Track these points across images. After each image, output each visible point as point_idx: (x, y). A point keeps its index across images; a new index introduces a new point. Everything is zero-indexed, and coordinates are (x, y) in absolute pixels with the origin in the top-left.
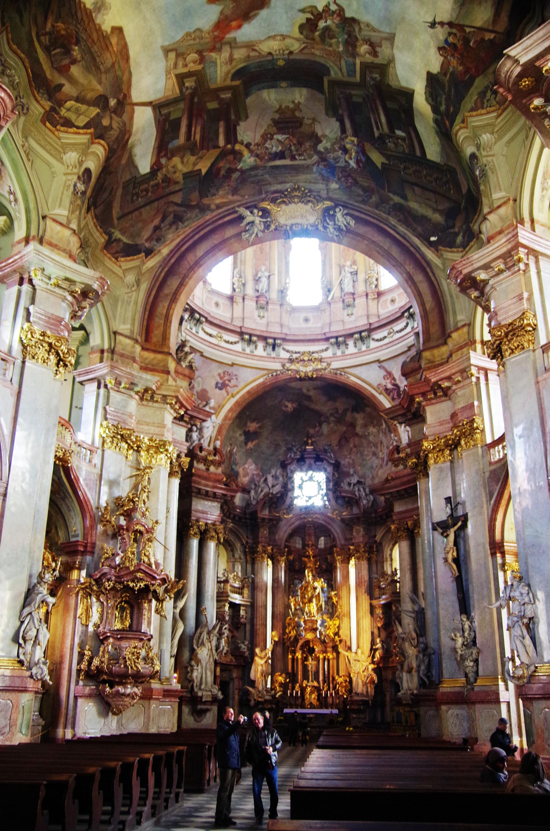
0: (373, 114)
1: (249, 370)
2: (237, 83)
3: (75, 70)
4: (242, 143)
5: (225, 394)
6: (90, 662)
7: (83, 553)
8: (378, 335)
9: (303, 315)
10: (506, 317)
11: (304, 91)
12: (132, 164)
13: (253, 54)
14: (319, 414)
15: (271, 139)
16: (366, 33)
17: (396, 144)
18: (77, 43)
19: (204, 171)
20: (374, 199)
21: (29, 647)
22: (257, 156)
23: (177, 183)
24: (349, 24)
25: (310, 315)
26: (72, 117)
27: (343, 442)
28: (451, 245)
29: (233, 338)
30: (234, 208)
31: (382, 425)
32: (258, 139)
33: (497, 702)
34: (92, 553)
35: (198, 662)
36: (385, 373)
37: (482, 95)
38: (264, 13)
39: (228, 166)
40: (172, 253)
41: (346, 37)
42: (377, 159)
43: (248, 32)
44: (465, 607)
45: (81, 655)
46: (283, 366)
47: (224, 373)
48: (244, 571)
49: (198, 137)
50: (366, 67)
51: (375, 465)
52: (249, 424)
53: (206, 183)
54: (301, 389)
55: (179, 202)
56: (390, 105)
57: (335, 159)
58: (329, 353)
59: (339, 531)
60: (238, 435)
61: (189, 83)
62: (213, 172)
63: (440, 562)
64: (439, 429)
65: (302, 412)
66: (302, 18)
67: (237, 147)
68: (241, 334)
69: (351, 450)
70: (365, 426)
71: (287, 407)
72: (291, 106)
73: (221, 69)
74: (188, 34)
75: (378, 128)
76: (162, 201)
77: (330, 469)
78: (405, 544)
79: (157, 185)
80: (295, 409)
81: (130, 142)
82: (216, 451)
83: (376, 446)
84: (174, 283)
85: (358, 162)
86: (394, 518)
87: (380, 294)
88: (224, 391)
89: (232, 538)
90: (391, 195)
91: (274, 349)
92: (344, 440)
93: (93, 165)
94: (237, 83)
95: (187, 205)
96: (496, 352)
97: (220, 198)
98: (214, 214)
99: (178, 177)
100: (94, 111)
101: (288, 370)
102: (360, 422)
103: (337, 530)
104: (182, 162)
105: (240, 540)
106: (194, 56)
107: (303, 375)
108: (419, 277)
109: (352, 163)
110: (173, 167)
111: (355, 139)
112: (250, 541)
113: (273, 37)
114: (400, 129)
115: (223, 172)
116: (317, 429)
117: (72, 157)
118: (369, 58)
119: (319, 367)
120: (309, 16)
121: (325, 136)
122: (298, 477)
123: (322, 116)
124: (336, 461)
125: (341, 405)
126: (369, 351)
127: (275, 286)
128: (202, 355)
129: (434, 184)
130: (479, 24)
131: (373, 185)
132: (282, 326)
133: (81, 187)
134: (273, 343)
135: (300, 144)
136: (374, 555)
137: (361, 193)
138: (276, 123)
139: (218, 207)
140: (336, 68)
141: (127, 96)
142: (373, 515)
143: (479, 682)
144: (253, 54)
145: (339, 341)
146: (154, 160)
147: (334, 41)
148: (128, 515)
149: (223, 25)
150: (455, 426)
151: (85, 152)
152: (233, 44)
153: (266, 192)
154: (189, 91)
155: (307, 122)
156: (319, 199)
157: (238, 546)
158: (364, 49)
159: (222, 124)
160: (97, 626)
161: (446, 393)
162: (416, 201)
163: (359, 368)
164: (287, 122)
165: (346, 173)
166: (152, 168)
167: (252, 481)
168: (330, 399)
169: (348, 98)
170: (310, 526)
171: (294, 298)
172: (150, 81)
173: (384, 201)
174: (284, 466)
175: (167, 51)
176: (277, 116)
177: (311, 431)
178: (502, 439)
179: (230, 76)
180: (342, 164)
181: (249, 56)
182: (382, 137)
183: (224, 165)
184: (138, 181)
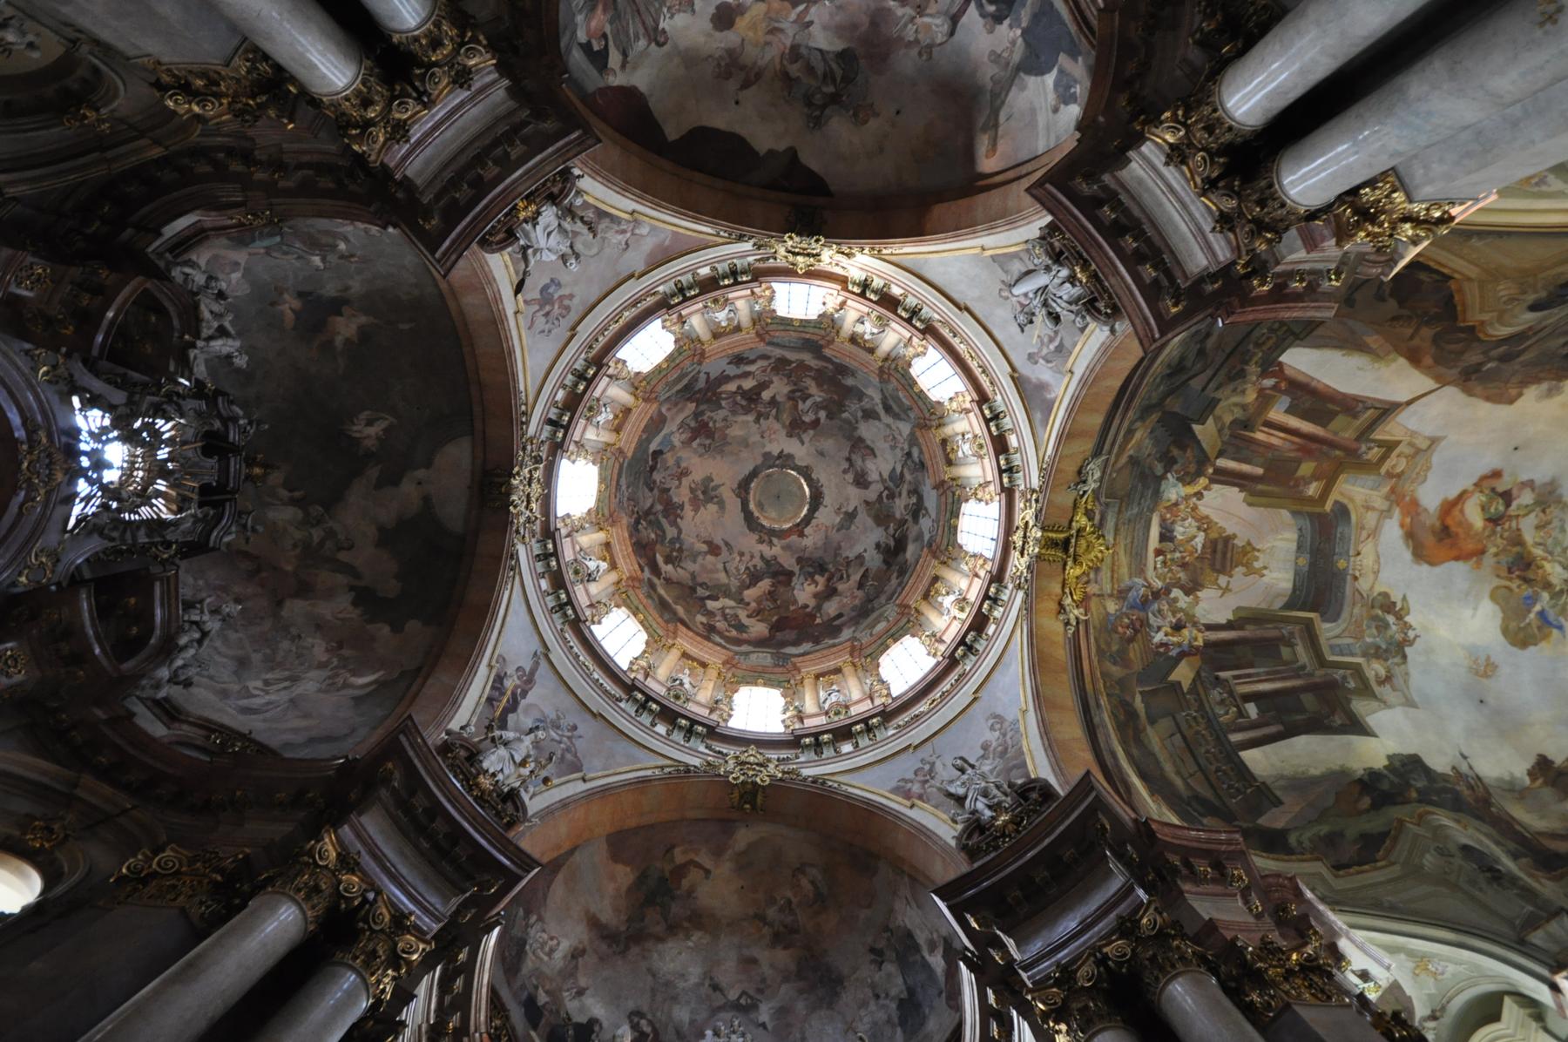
0: (1268, 673)
1: (547, 365)
2: (1328, 506)
4: (1206, 488)
5: (529, 297)
13: (1364, 534)
14: (333, 500)
15: (1199, 528)
16: (1397, 671)
17: (1222, 702)
19: (1196, 428)
20: (1116, 671)
22: (1176, 504)
23: (1217, 389)
24: (1398, 649)
30: (1110, 453)
31: (355, 674)
39: (1181, 461)
41: (1384, 646)
42: (1183, 674)
43: (1392, 531)
46: (531, 440)
47: (568, 308)
49: (1259, 436)
50: (1357, 670)
52: (363, 319)
54: (428, 464)
55: (1192, 382)
57: (1159, 611)
60: (351, 283)
66: (1396, 597)
67: (1203, 481)
70: (319, 626)
71: (370, 423)
72: (1257, 565)
74: (1429, 468)
75: (1236, 677)
79: (1247, 363)
81: (1402, 361)
85: (1162, 645)
86: (346, 830)
90: (1138, 699)
91: (550, 422)
94: (1328, 506)
97: (1142, 439)
98: (1126, 424)
99: (1218, 395)
101: (524, 449)
102: (326, 610)
104: (1236, 405)
106: (1402, 465)
107: (515, 482)
109: (1159, 637)
110: (1243, 392)
111: (1200, 643)
114: (1261, 711)
115: (1175, 452)
116: (284, 493)
118: (1370, 674)
120: (1399, 606)
121: (1197, 600)
124: (213, 549)
128: (632, 276)
129: (1213, 768)
131: (1138, 666)
135: (1184, 566)
137: (1115, 648)
138: (1228, 540)
139: (1130, 432)
140: (1337, 631)
144: (1364, 534)
146: (1287, 372)
147: (1374, 631)
149: (1412, 508)
152: (1386, 514)
153: (1107, 505)
154: (1364, 448)
155: (1223, 580)
159: (1260, 471)
162: (1162, 740)
163: (524, 607)
164: (1223, 554)
165: (1141, 628)
166: (1280, 364)
168: (381, 529)
173: (1121, 682)
175: (1434, 441)
176: (1239, 542)
177: (276, 477)
179: (1345, 501)
180: (1152, 620)
181: (1363, 528)
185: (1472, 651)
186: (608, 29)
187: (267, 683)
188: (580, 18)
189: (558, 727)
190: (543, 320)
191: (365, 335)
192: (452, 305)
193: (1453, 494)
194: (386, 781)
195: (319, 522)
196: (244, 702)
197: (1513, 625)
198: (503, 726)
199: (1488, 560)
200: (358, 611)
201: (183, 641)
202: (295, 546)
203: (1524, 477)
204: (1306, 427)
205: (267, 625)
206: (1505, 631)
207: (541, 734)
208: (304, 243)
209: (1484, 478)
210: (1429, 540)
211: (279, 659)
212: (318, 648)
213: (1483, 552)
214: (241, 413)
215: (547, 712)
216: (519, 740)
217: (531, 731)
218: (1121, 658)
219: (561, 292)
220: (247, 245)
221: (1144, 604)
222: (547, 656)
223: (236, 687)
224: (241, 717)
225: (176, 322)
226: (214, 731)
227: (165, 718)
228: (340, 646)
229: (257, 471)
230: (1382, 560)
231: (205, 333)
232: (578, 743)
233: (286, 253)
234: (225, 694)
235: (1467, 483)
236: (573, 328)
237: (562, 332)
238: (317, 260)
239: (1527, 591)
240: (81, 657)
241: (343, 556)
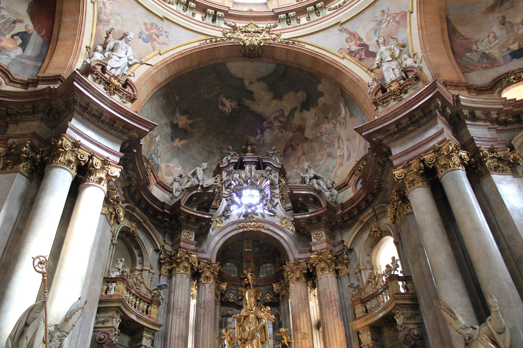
1: (183, 30)
14: (260, 118)
27: (289, 151)
31: (340, 114)
36: (348, 36)
46: (224, 34)
47: (152, 24)
51: (331, 168)
52: (178, 115)
54: (242, 80)
59: (292, 243)
60: (163, 123)
69: (299, 158)
70: (317, 125)
71: (224, 105)
77: (275, 176)
80: (233, 110)
83: (331, 145)
86: (395, 163)
88: (149, 45)
91: (214, 20)
92: (289, 149)
101: (230, 38)
105: (153, 242)
107: (248, 43)
112: (168, 248)
116: (258, 137)
119: (268, 37)
124: (282, 166)
125: (289, 101)
142: (340, 212)
157: (150, 250)
163: (315, 36)
168: (274, 98)
177: (252, 140)
186: (8, 36)
187: (339, 148)
188: (13, 56)
189: (381, 22)
190: (161, 37)
191: (184, 113)
192: (163, 85)
194: (380, 141)
195: (271, 123)
196: (345, 158)
198: (373, 55)
200: (312, 109)
201: (316, 186)
202: (282, 132)
205: (315, 144)
207: (381, 41)
208: (152, 145)
211: (330, 142)
212: (327, 126)
214: (226, 158)
215: (371, 28)
216: (382, 53)
217: (378, 44)
219: (144, 30)
220: (158, 165)
222: (342, 24)
223: (339, 159)
224: (351, 161)
225: (195, 192)
226: (354, 172)
227: (346, 188)
228: (327, 118)
229: (249, 148)
231: (197, 182)
232: (392, 11)
233: (158, 150)
234: (341, 164)
236: (162, 19)
238: (157, 139)
240: (318, 218)
241: (286, 114)
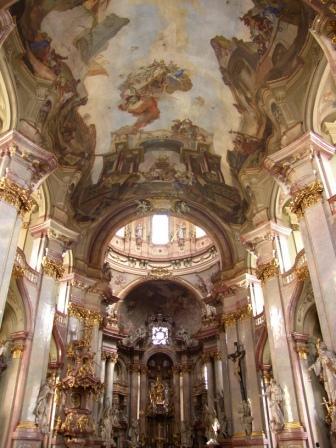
3: (72, 141)
6: (60, 426)
7: (57, 368)
8: (196, 260)
9: (158, 249)
10: (266, 260)
11: (171, 152)
12: (90, 180)
16: (201, 132)
18: (75, 130)
20: (200, 199)
21: (40, 417)
24: (193, 128)
25: (162, 249)
26: (69, 161)
28: (236, 222)
29: (125, 259)
32: (148, 170)
33: (263, 444)
34: (62, 368)
35: (104, 426)
37: (252, 162)
38: (156, 121)
40: (104, 220)
42: (202, 182)
43: (148, 128)
44: (245, 398)
45: (56, 422)
48: (126, 378)
50: (200, 145)
53: (122, 188)
56: (210, 161)
58: (171, 268)
61: (121, 147)
62: (125, 184)
63: (232, 374)
64: (230, 309)
65: (155, 298)
66: (173, 124)
68: (128, 257)
73: (135, 142)
76: (101, 197)
78: (209, 364)
82: (115, 316)
84: (103, 234)
87: (196, 240)
89: (121, 361)
93: (75, 182)
95: (112, 199)
96: (261, 277)
97: (127, 195)
99: (110, 186)
100: (79, 158)
103: (173, 357)
108: (220, 236)
109: (191, 183)
113: (158, 131)
117: (67, 178)
122: (154, 329)
123: (179, 163)
125: (176, 293)
126: (192, 267)
127: (145, 234)
130: (250, 134)
132: (148, 253)
133: (70, 192)
134: (143, 262)
135: (167, 173)
136: (191, 369)
139: (127, 199)
141: (93, 152)
143: (253, 434)
145: (176, 262)
148: (81, 349)
149: (138, 125)
150: (238, 309)
151: (72, 177)
152: (142, 132)
156: (174, 197)
158: (200, 138)
160: (64, 406)
161: (234, 292)
164: (162, 164)
165: (187, 186)
167: (131, 331)
169: (191, 156)
170: (160, 356)
171: (155, 240)
172: (104, 146)
173: (204, 200)
174: (147, 324)
178: (261, 314)
182: (205, 174)
183: (131, 181)
184: (92, 188)
185: (193, 103)
193: (131, 115)
197: (183, 87)
199: (155, 95)
203: (120, 98)
204: (115, 164)
206: (185, 90)
209: (122, 109)
210: (149, 115)
213: (153, 99)
218: (198, 196)
221: (179, 184)
230: (159, 128)
235: (126, 114)
237: (125, 275)
239: (167, 81)
